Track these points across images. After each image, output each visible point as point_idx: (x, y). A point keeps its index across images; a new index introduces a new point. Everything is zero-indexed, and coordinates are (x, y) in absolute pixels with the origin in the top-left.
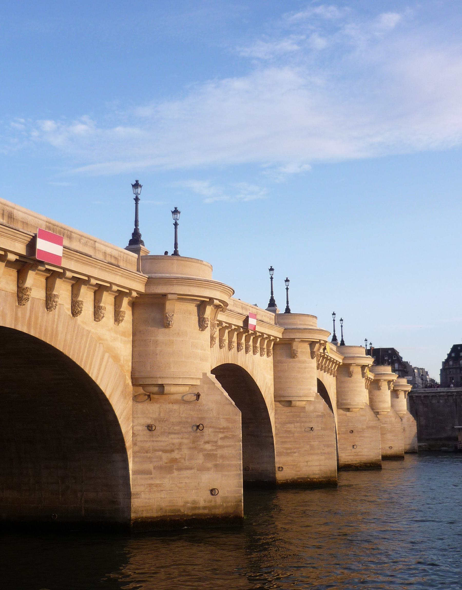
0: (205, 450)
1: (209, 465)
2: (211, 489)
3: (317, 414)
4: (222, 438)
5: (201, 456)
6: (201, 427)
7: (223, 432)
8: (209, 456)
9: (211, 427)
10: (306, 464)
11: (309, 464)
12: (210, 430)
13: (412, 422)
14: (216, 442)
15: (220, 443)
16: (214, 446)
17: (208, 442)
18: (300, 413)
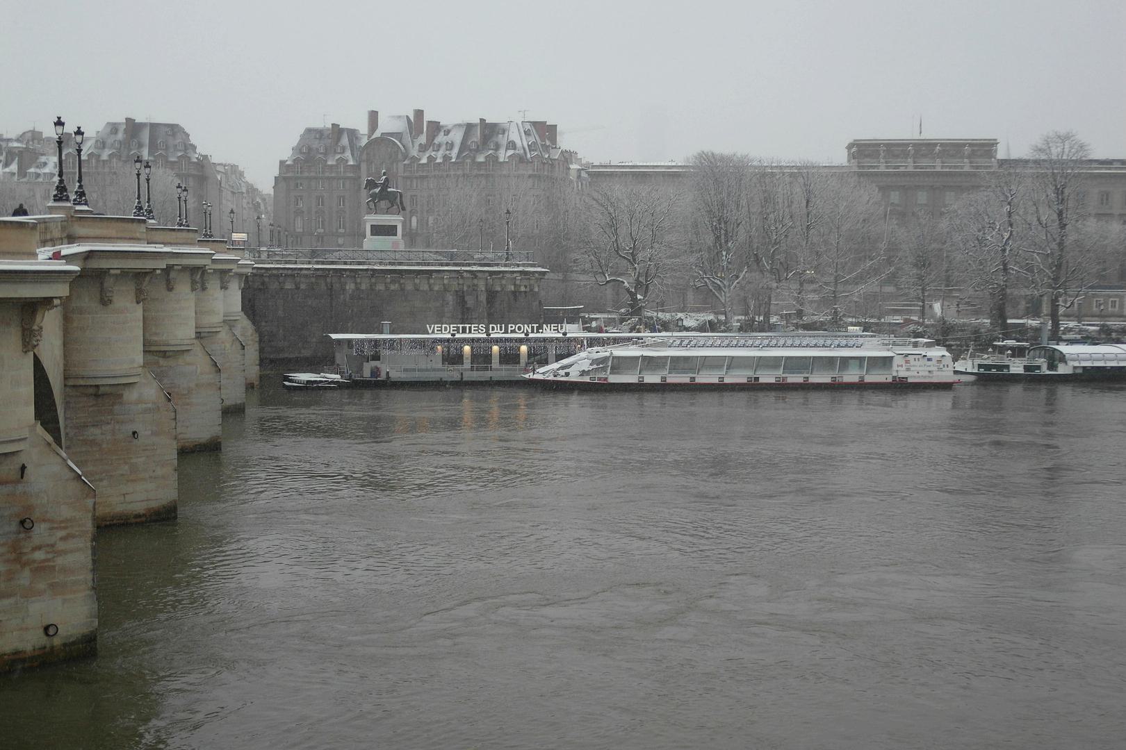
0: (34, 561)
1: (42, 586)
2: (44, 625)
3: (144, 406)
4: (63, 539)
5: (27, 573)
6: (27, 525)
7: (65, 528)
8: (41, 569)
9: (44, 521)
10: (122, 498)
11: (128, 498)
12: (43, 526)
13: (252, 335)
14: (53, 546)
15: (61, 546)
16: (48, 553)
17: (39, 548)
18: (112, 406)
